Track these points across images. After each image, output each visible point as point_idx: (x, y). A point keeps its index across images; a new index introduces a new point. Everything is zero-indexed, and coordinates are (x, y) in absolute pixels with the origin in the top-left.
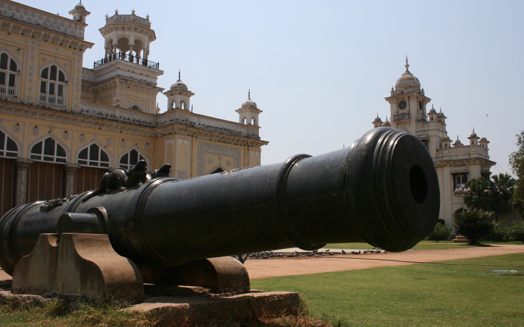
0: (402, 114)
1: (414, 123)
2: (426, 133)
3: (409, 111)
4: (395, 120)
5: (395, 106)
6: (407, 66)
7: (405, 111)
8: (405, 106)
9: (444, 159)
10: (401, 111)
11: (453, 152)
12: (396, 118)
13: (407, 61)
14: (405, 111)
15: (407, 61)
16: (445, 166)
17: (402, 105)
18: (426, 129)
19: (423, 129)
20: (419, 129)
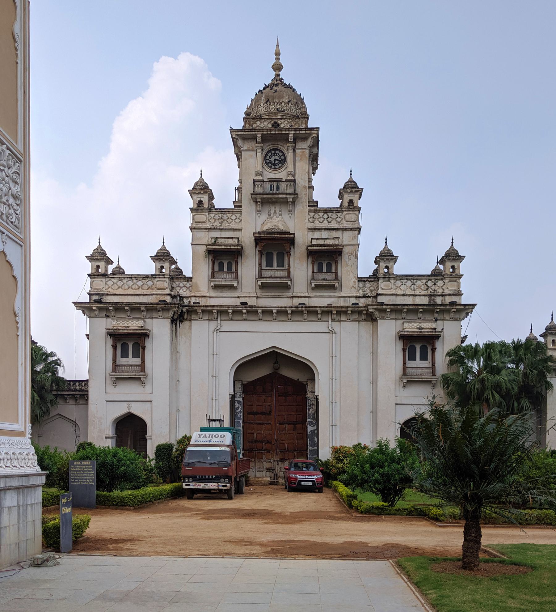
0: (271, 181)
1: (307, 209)
2: (334, 234)
3: (294, 176)
4: (254, 196)
5: (255, 159)
6: (278, 67)
7: (282, 174)
8: (283, 161)
9: (380, 299)
10: (269, 174)
11: (403, 287)
12: (259, 190)
13: (278, 54)
14: (282, 174)
15: (278, 54)
16: (383, 318)
17: (274, 160)
18: (334, 225)
19: (325, 225)
20: (318, 225)
